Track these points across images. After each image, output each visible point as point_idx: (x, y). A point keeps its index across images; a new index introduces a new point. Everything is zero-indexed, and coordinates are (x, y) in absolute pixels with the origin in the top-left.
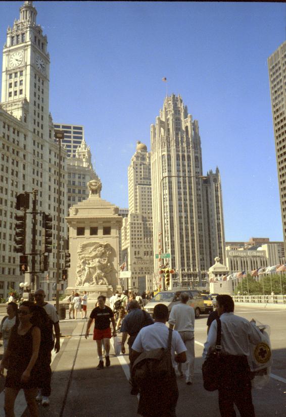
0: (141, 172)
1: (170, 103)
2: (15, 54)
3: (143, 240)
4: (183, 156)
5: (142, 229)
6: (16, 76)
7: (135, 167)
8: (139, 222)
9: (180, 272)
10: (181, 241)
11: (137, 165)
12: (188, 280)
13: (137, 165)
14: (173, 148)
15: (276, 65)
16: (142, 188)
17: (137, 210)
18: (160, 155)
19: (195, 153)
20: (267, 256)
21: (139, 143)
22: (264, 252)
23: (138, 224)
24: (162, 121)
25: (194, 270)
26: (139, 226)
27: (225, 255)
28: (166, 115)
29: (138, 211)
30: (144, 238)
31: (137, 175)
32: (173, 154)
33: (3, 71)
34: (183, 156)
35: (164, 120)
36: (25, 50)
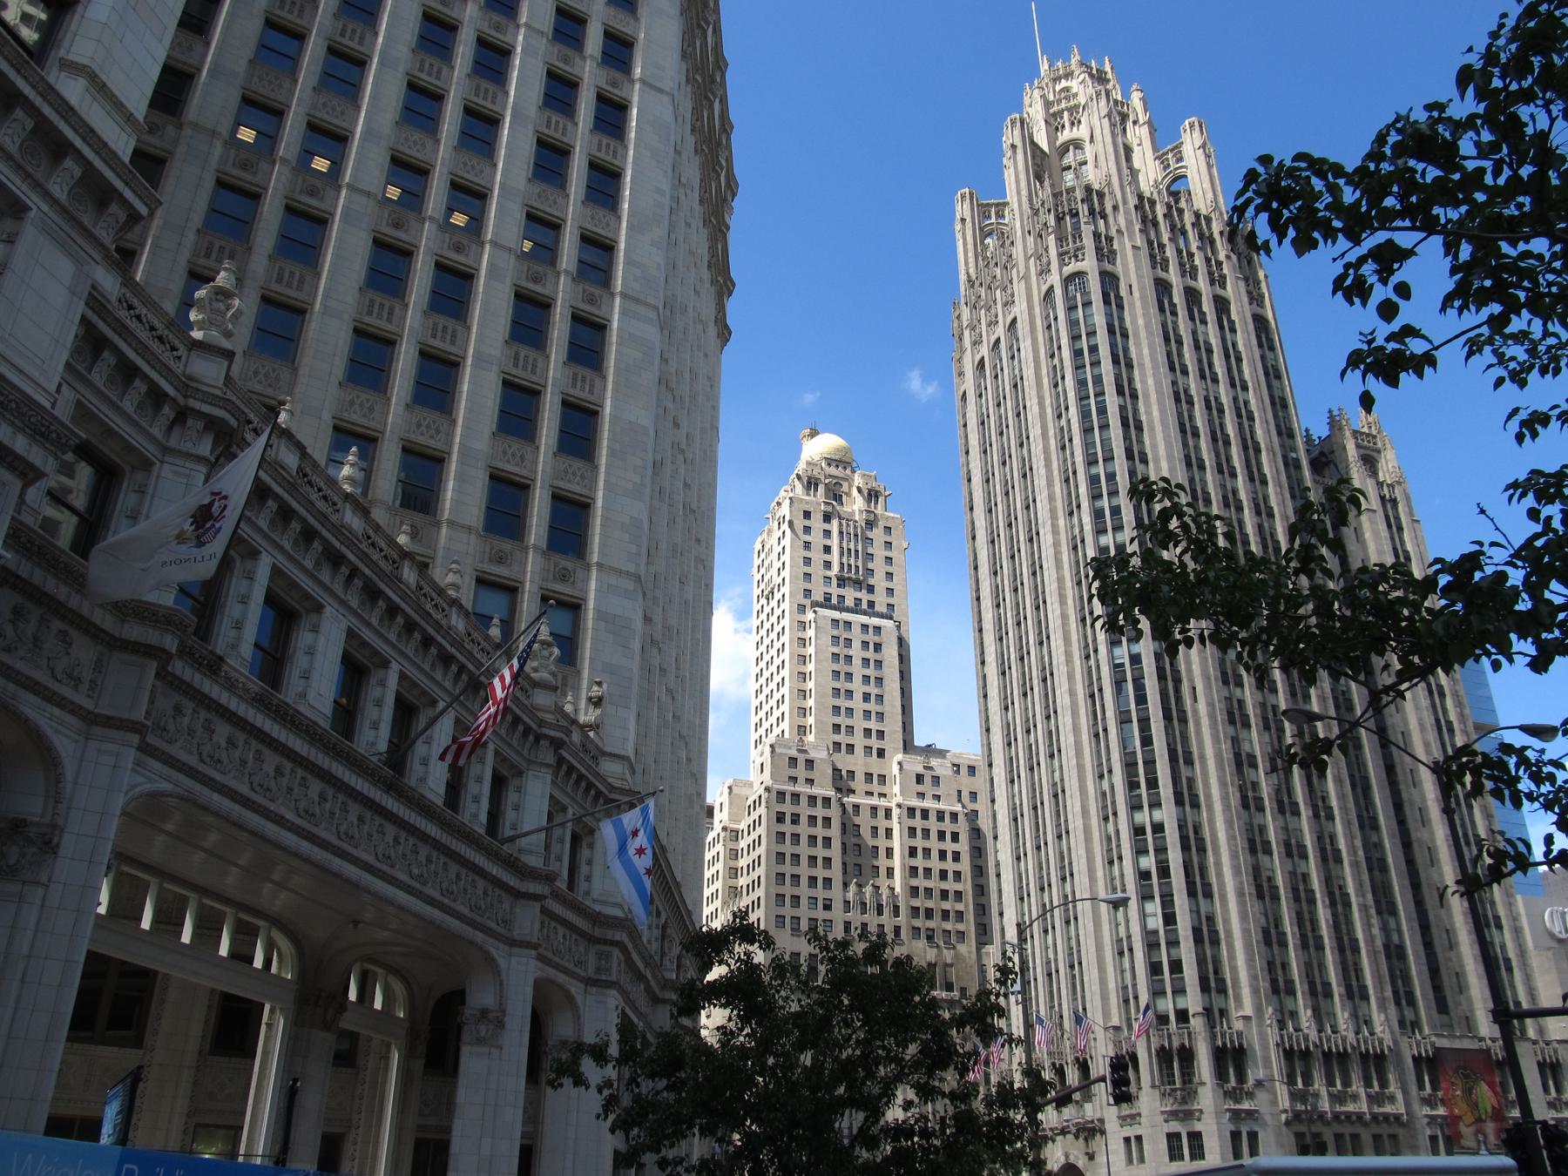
0: (827, 549)
3: (836, 893)
4: (1192, 296)
5: (835, 832)
7: (800, 523)
8: (815, 791)
9: (1273, 1036)
11: (807, 515)
13: (807, 515)
16: (835, 622)
17: (802, 730)
18: (1055, 279)
21: (814, 433)
23: (812, 799)
25: (1361, 1021)
26: (819, 812)
27: (1517, 931)
29: (811, 738)
30: (846, 885)
31: (807, 561)
34: (1192, 296)
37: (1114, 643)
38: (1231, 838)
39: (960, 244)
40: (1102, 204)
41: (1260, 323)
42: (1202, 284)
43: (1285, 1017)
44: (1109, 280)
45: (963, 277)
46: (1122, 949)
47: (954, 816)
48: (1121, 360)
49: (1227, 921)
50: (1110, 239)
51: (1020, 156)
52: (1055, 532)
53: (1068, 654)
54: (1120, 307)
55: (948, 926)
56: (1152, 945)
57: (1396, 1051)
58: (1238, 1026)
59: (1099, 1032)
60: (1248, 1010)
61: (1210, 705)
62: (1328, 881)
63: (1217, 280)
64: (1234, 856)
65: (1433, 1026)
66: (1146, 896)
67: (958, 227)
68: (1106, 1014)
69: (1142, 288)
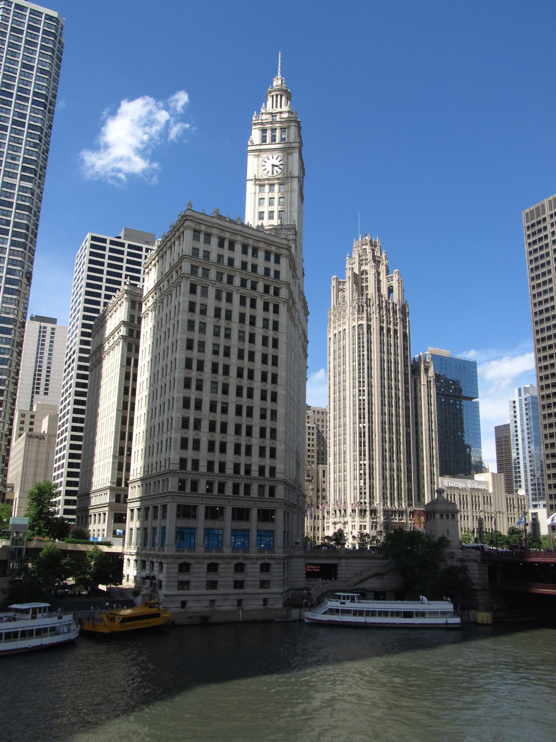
1: (365, 249)
2: (270, 157)
4: (389, 330)
6: (271, 190)
9: (382, 507)
10: (383, 460)
12: (400, 520)
14: (375, 317)
15: (539, 222)
18: (355, 324)
19: (405, 327)
20: (491, 491)
22: (486, 483)
24: (354, 273)
25: (400, 504)
28: (360, 265)
32: (375, 325)
33: (248, 178)
34: (389, 330)
35: (357, 273)
36: (289, 154)
37: (360, 423)
38: (379, 468)
39: (332, 293)
40: (370, 302)
41: (405, 335)
42: (391, 326)
43: (385, 503)
44: (369, 327)
45: (332, 306)
46: (355, 488)
47: (313, 428)
48: (369, 350)
49: (376, 485)
50: (370, 314)
51: (351, 280)
52: (350, 392)
53: (350, 422)
54: (371, 334)
55: (309, 459)
56: (361, 489)
57: (406, 510)
58: (375, 505)
59: (349, 505)
60: (378, 502)
61: (379, 438)
62: (398, 476)
63: (395, 325)
64: (379, 471)
65: (415, 505)
66: (360, 479)
67: (332, 288)
68: (351, 501)
69: (376, 330)
